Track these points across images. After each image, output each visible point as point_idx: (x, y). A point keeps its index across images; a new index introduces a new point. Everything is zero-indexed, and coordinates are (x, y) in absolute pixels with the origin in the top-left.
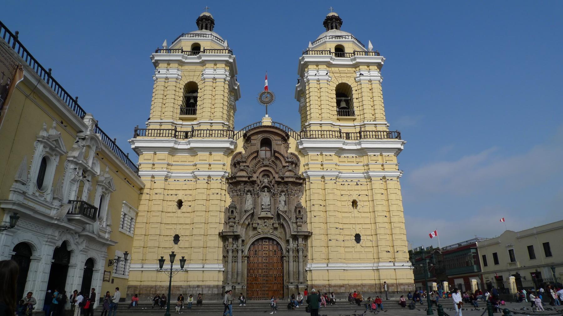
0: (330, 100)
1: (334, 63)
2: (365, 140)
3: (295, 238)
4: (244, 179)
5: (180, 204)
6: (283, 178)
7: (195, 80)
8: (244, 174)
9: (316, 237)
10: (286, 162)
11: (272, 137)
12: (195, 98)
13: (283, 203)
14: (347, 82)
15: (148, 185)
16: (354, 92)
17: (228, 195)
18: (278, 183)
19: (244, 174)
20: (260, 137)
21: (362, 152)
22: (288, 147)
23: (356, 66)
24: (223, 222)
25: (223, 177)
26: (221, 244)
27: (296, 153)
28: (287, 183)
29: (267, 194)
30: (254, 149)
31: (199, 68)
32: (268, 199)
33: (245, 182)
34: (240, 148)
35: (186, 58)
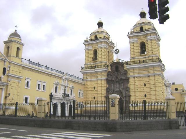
0: (138, 49)
1: (138, 35)
2: (147, 63)
3: (125, 97)
4: (110, 80)
5: (95, 88)
6: (121, 79)
7: (96, 48)
8: (110, 78)
9: (132, 96)
10: (122, 73)
11: (118, 65)
12: (97, 54)
13: (122, 86)
14: (143, 41)
15: (86, 83)
16: (146, 45)
17: (107, 85)
18: (121, 80)
19: (110, 78)
20: (115, 66)
21: (148, 67)
22: (124, 68)
23: (147, 34)
24: (106, 93)
25: (105, 79)
26: (106, 99)
27: (127, 69)
28: (123, 80)
29: (118, 83)
30: (113, 70)
31: (97, 44)
32: (118, 85)
33: (111, 81)
34: (110, 70)
35: (93, 42)
